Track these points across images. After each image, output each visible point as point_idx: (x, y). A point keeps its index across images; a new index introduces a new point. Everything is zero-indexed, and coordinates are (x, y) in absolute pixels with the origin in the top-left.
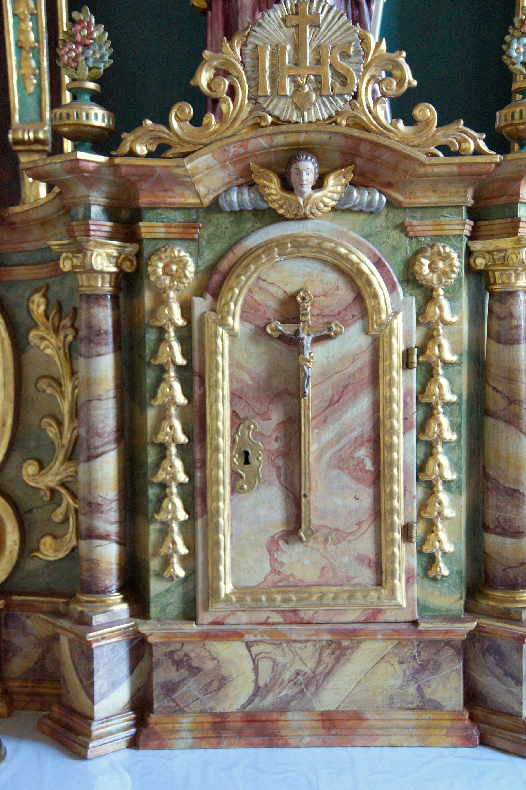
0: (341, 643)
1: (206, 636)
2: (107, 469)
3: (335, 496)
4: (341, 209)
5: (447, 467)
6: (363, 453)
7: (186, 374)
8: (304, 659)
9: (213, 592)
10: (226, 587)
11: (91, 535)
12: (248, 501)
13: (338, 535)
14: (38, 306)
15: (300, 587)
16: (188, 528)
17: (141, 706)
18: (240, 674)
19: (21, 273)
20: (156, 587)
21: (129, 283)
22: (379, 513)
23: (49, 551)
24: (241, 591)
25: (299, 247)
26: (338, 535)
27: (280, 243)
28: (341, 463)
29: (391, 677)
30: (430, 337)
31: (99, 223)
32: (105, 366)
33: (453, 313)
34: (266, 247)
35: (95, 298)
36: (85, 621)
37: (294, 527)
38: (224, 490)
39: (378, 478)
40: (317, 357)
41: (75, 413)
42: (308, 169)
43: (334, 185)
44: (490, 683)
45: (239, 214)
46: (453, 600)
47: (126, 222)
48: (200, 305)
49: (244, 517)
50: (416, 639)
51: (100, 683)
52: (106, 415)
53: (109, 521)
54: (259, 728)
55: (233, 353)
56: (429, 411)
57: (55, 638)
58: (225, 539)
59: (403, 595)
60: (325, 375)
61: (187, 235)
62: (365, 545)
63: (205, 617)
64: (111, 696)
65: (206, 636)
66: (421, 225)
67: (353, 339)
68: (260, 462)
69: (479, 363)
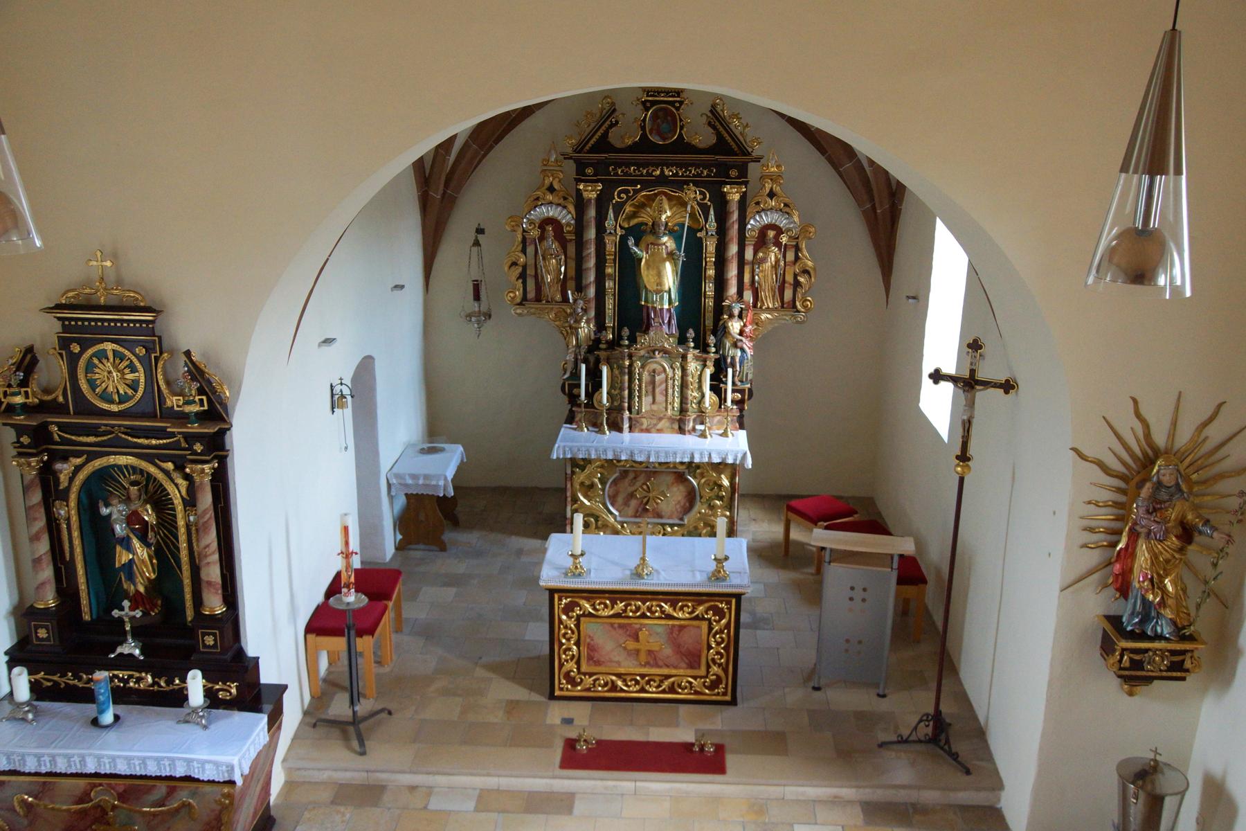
0: (660, 419)
2: (626, 392)
3: (660, 398)
8: (655, 421)
17: (630, 427)
21: (631, 365)
29: (668, 424)
33: (679, 373)
37: (654, 402)
39: (666, 396)
40: (657, 378)
47: (630, 356)
49: (646, 401)
50: (672, 420)
52: (626, 385)
54: (648, 431)
55: (646, 376)
59: (669, 412)
64: (626, 426)
67: (663, 375)
69: (682, 377)
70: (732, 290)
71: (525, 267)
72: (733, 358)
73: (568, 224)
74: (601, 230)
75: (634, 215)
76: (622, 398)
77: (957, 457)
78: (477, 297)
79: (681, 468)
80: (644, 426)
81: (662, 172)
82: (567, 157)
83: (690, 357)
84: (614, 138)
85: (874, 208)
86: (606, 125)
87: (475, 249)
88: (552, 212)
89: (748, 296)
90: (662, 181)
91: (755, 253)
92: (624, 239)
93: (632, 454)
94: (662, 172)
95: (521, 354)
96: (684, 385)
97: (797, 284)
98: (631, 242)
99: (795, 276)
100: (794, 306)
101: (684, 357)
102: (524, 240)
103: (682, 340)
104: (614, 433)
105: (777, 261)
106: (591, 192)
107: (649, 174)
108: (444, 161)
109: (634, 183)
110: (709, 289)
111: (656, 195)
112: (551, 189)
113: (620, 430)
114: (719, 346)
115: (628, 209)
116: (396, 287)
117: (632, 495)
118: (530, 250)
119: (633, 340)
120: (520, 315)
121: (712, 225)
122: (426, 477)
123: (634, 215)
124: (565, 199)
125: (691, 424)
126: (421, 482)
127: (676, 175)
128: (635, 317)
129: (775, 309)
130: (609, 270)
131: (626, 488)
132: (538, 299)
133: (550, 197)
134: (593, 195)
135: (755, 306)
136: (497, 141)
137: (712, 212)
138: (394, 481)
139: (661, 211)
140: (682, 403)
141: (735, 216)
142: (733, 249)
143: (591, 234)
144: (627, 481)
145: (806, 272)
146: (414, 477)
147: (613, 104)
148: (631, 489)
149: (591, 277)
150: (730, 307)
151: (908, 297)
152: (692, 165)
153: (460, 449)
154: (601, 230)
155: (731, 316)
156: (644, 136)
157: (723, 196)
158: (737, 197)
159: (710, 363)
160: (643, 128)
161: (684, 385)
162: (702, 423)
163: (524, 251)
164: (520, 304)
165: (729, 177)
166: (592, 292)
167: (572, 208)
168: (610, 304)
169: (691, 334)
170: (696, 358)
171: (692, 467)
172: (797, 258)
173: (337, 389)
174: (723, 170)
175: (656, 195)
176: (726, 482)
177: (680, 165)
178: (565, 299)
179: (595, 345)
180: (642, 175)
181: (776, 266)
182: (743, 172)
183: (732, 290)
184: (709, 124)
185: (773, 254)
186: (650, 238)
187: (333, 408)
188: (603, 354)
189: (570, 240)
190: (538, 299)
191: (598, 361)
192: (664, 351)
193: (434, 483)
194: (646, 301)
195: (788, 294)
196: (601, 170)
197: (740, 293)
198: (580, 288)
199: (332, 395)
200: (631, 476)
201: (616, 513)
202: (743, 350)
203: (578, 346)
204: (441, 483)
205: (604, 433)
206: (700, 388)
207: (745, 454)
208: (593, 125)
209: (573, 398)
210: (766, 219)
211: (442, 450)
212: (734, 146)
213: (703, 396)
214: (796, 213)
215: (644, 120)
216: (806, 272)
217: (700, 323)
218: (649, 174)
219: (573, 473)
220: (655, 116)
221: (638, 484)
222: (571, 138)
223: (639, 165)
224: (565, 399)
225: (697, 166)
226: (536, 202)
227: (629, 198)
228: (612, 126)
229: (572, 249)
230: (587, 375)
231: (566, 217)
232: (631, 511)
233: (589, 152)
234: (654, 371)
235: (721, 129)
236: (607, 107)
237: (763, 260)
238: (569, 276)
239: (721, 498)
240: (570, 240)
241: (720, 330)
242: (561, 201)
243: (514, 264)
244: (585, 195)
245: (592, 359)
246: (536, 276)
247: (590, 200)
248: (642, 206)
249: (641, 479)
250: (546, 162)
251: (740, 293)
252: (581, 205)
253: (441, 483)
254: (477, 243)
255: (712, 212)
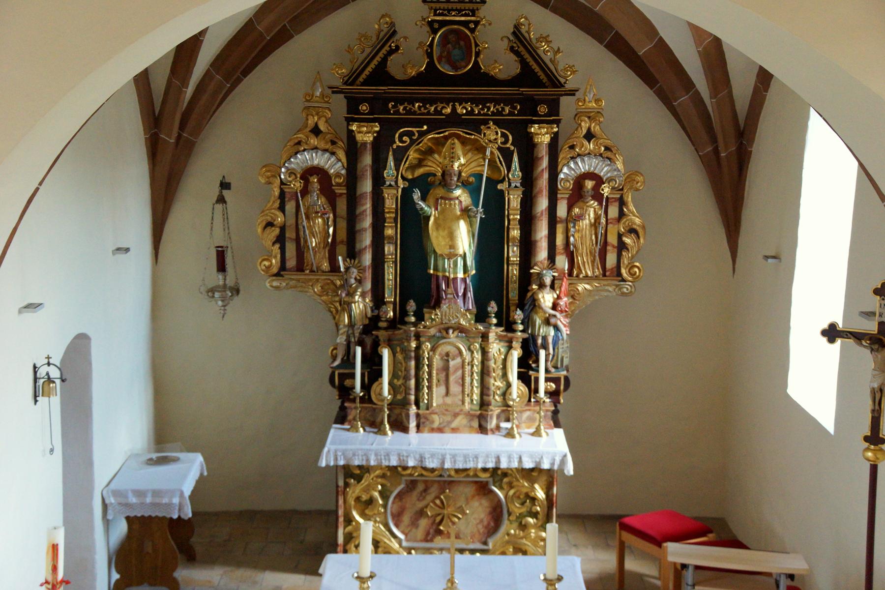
0: (456, 415)
1: (430, 414)
2: (413, 382)
3: (455, 388)
4: (457, 337)
5: (475, 384)
6: (460, 381)
7: (428, 366)
8: (449, 418)
9: (432, 405)
10: (434, 405)
11: (410, 394)
12: (439, 389)
13: (455, 395)
14: (398, 349)
15: (448, 405)
16: (428, 394)
17: (418, 426)
18: (437, 420)
19: (395, 342)
20: (421, 404)
21: (418, 348)
22: (463, 392)
23: (399, 397)
24: (437, 405)
25: (449, 343)
26: (455, 395)
27: (446, 343)
28: (456, 382)
30: (473, 360)
31: (413, 338)
32: (413, 363)
33: (478, 356)
34: (443, 343)
35: (411, 351)
36: (408, 410)
38: (434, 386)
39: (463, 385)
40: (452, 363)
41: (405, 370)
42: (451, 331)
43: (456, 333)
44: (483, 423)
45: (438, 338)
46: (477, 408)
47: (418, 337)
48: (431, 353)
49: (438, 392)
50: (470, 416)
51: (411, 421)
52: (413, 372)
53: (413, 392)
54: (440, 430)
55: (437, 361)
56: (472, 373)
57: (401, 414)
58: (434, 395)
59: (467, 406)
60: (454, 366)
61: (429, 341)
62: (460, 397)
63: (430, 410)
64: (413, 424)
65: (430, 414)
66: (471, 340)
67: (459, 360)
68: (441, 381)
69: (483, 363)
70: (542, 254)
71: (283, 229)
72: (545, 338)
73: (338, 175)
74: (378, 181)
75: (420, 163)
76: (407, 389)
77: (866, 439)
78: (222, 267)
79: (484, 476)
80: (436, 425)
81: (454, 109)
82: (336, 91)
83: (491, 335)
84: (394, 67)
85: (716, 151)
86: (384, 51)
87: (219, 207)
88: (318, 159)
89: (562, 262)
90: (454, 120)
91: (570, 208)
92: (407, 194)
93: (422, 459)
94: (454, 109)
95: (277, 338)
96: (485, 372)
97: (622, 247)
98: (417, 195)
99: (620, 236)
100: (619, 274)
101: (485, 337)
102: (282, 195)
103: (481, 316)
104: (398, 434)
105: (597, 218)
106: (366, 134)
107: (437, 112)
108: (180, 92)
109: (418, 123)
110: (513, 253)
111: (446, 138)
112: (316, 131)
113: (405, 429)
114: (528, 322)
115: (412, 155)
116: (118, 249)
117: (421, 513)
118: (290, 207)
119: (420, 317)
120: (277, 288)
121: (516, 173)
122: (156, 493)
123: (420, 163)
124: (333, 143)
125: (494, 422)
126: (148, 500)
127: (471, 113)
128: (422, 288)
129: (596, 278)
130: (389, 232)
131: (413, 503)
132: (300, 267)
133: (314, 141)
134: (369, 138)
135: (570, 274)
136: (246, 72)
137: (516, 158)
138: (111, 500)
139: (453, 158)
140: (482, 394)
141: (545, 163)
142: (543, 204)
143: (367, 186)
144: (415, 494)
145: (632, 231)
146: (139, 493)
147: (392, 24)
148: (420, 505)
149: (366, 240)
150: (540, 276)
151: (767, 257)
152: (491, 101)
153: (199, 458)
154: (378, 181)
155: (542, 286)
156: (431, 65)
157: (530, 137)
158: (547, 139)
159: (517, 345)
160: (430, 55)
161: (485, 372)
162: (508, 420)
163: (282, 208)
164: (278, 275)
165: (536, 114)
166: (367, 259)
167: (342, 155)
168: (390, 274)
169: (493, 307)
170: (500, 338)
171: (498, 474)
172: (622, 214)
173: (42, 372)
174: (529, 107)
175: (446, 138)
176: (540, 494)
177: (475, 101)
178: (334, 268)
179: (372, 323)
180: (429, 113)
181: (595, 224)
182: (554, 108)
183: (542, 254)
184: (512, 49)
185: (592, 210)
186: (440, 192)
187: (35, 396)
188: (382, 335)
189: (341, 194)
190: (300, 267)
191: (376, 344)
192: (460, 329)
193: (165, 500)
194: (436, 269)
195: (611, 259)
196: (378, 105)
197: (552, 257)
198: (353, 254)
199: (36, 380)
200: (420, 487)
201: (401, 536)
202: (557, 328)
203: (351, 325)
204: (176, 501)
205: (385, 434)
206: (505, 375)
207: (565, 456)
208: (368, 50)
209: (345, 392)
210: (583, 166)
211: (176, 460)
212: (543, 77)
213: (509, 385)
214: (620, 158)
215: (431, 45)
216: (632, 231)
217: (503, 294)
218: (437, 112)
219: (347, 485)
220: (444, 37)
221: (429, 498)
222: (341, 66)
223: (427, 100)
224: (335, 393)
225: (497, 102)
226: (298, 147)
227: (413, 142)
228: (391, 52)
229: (342, 206)
230: (363, 362)
231: (335, 165)
232: (420, 533)
233: (363, 84)
234: (447, 355)
235: (527, 56)
236: (385, 28)
237: (580, 217)
238: (338, 239)
239: (535, 515)
240: (341, 194)
241: (528, 304)
242: (329, 146)
243: (270, 224)
244: (359, 137)
245: (368, 341)
246: (297, 240)
247: (364, 144)
248: (430, 152)
249: (434, 491)
250: (309, 97)
251: (552, 257)
252: (353, 150)
253: (176, 501)
254: (221, 200)
255: (516, 158)
